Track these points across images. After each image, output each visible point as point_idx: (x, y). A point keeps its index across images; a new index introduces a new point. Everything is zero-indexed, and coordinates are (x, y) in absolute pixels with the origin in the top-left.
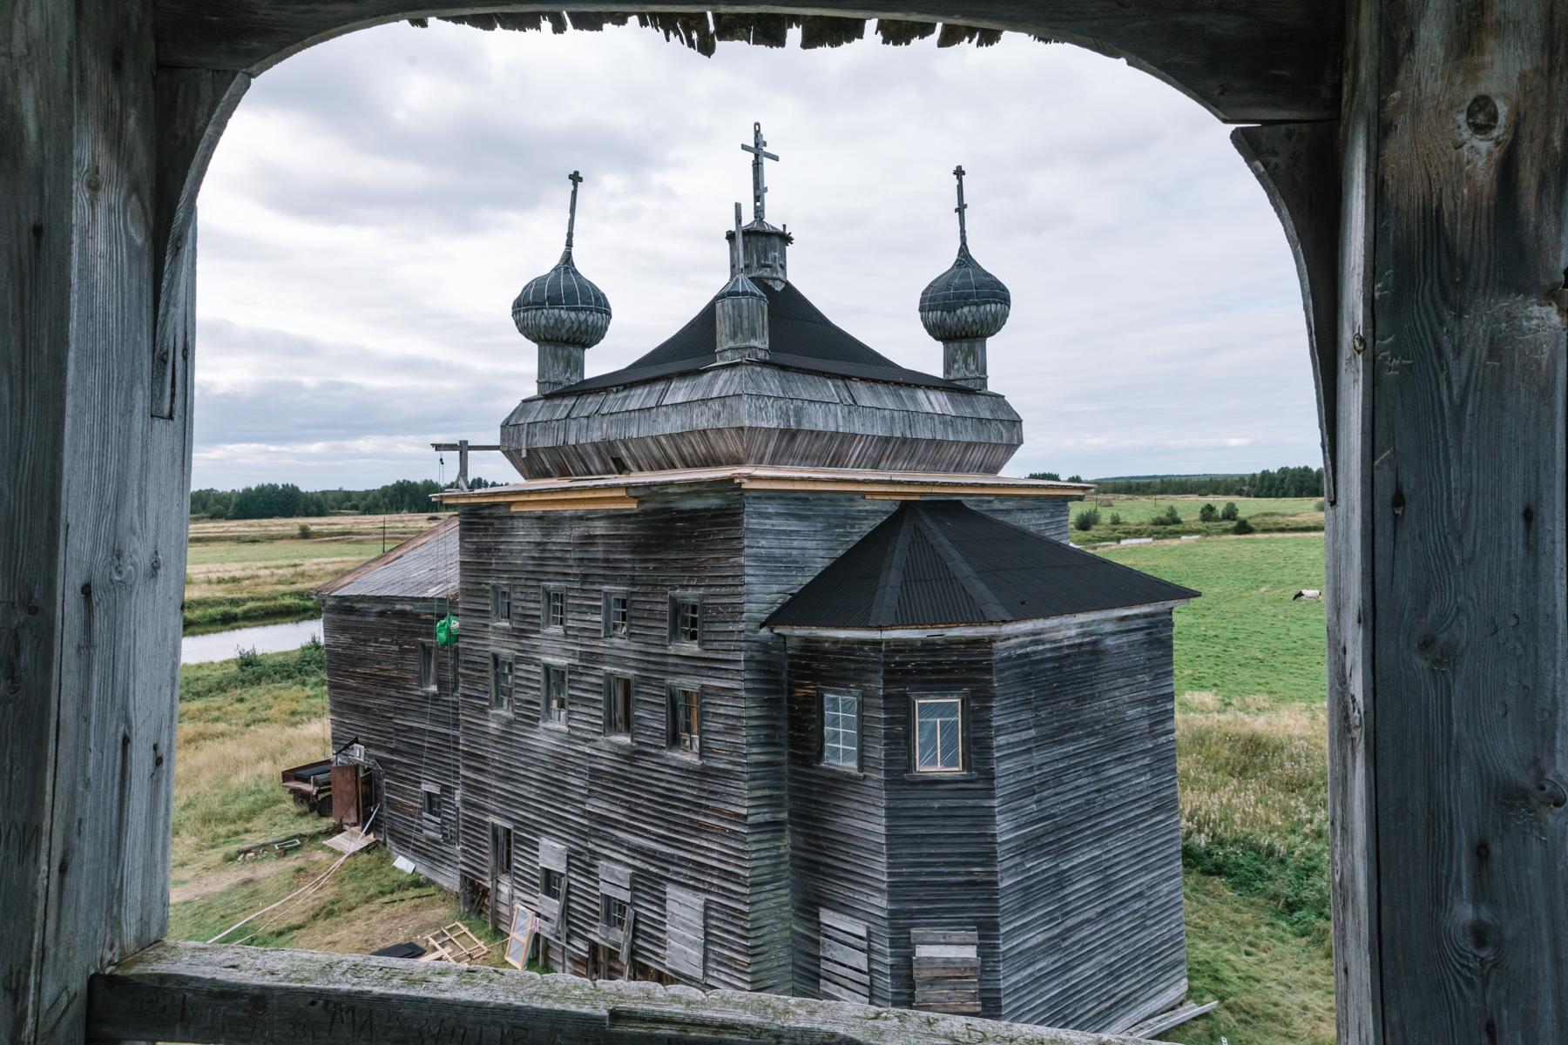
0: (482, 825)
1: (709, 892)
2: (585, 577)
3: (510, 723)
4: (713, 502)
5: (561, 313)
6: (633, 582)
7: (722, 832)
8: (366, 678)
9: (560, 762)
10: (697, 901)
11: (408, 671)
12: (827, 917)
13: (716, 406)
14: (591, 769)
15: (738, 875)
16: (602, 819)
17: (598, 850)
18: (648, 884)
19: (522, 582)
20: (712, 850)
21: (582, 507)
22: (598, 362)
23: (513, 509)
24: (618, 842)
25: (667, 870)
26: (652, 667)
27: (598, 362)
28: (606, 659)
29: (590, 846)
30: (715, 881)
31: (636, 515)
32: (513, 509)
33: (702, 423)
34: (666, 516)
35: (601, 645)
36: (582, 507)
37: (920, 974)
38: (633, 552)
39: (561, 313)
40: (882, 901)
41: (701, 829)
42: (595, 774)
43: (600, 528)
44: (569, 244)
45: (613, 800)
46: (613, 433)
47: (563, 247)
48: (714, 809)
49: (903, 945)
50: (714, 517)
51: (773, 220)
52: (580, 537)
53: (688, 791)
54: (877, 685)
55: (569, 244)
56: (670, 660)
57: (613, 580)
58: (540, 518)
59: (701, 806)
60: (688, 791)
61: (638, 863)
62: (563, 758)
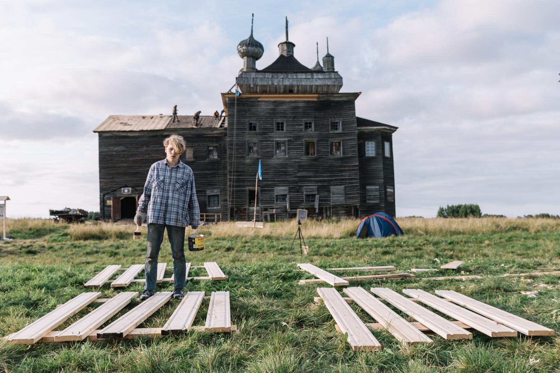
0: (244, 191)
2: (294, 117)
4: (345, 99)
5: (252, 49)
6: (315, 117)
7: (350, 170)
8: (136, 162)
9: (284, 166)
10: (343, 186)
12: (368, 187)
13: (334, 80)
18: (324, 188)
20: (346, 175)
21: (293, 100)
22: (261, 64)
23: (259, 99)
24: (311, 181)
27: (261, 64)
32: (259, 99)
33: (329, 83)
35: (302, 134)
37: (388, 194)
39: (252, 49)
40: (382, 180)
41: (345, 171)
42: (300, 166)
43: (301, 105)
44: (252, 32)
45: (309, 171)
46: (295, 83)
47: (250, 33)
49: (386, 188)
51: (290, 40)
54: (380, 138)
55: (252, 32)
57: (308, 117)
60: (338, 164)
62: (286, 164)
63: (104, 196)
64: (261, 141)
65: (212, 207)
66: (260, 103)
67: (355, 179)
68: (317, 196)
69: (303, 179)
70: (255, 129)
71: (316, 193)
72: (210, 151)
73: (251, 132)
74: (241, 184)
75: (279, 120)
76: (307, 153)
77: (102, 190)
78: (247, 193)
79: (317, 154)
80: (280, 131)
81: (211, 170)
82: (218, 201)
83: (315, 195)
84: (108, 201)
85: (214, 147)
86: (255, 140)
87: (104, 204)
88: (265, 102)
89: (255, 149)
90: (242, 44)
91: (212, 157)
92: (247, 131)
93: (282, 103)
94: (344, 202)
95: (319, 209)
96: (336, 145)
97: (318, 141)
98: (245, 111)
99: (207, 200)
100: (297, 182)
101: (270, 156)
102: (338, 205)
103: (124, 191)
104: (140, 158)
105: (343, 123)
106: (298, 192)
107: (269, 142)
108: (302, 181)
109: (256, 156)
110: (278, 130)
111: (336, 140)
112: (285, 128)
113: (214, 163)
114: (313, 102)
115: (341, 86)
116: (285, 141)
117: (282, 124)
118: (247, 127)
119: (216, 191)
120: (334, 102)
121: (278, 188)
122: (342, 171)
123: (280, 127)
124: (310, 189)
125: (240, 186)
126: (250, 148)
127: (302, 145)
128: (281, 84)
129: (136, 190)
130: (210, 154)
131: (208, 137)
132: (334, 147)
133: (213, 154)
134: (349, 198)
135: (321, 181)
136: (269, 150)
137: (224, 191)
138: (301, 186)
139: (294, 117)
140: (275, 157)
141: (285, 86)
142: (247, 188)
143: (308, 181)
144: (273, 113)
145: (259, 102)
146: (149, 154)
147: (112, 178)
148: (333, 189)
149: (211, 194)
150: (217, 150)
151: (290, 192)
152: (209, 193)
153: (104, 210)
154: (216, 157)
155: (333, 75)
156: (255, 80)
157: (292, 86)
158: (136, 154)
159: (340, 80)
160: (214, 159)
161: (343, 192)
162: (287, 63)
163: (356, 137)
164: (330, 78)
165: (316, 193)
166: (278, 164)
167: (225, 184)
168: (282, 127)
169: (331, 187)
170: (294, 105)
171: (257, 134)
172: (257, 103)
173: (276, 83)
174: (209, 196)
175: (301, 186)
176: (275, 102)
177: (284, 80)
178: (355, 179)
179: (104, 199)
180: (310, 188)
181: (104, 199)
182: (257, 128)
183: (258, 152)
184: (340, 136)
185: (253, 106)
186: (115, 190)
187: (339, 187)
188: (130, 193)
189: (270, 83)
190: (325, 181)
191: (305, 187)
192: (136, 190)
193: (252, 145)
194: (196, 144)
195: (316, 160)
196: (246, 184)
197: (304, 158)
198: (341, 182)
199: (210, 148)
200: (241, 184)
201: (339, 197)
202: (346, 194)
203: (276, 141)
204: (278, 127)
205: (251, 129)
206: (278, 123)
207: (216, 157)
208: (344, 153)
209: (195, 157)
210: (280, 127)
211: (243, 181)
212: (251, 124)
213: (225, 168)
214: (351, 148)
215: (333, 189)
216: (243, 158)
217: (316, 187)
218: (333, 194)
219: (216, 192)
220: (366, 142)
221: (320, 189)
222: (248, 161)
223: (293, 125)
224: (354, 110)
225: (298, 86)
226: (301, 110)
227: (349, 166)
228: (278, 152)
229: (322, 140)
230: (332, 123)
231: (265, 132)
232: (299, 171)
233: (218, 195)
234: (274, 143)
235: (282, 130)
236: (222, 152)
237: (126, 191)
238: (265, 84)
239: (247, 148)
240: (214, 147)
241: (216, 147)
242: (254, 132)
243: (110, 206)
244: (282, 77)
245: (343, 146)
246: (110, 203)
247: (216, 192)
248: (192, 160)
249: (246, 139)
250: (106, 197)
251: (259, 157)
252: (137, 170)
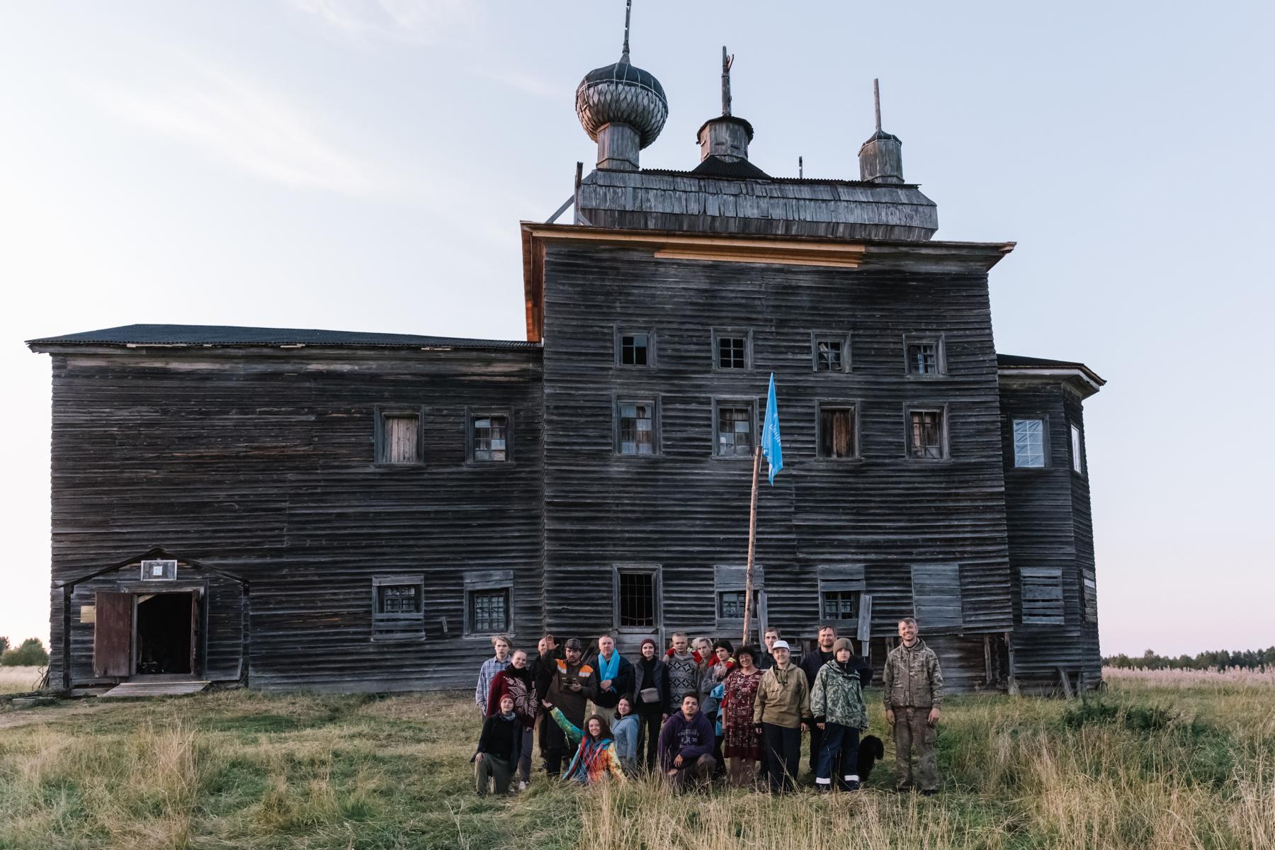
1: (960, 559)
2: (782, 323)
3: (653, 463)
4: (952, 268)
6: (854, 326)
10: (955, 566)
11: (341, 445)
14: (797, 489)
15: (995, 538)
16: (815, 529)
17: (813, 557)
19: (675, 326)
20: (965, 526)
21: (777, 262)
25: (911, 553)
26: (885, 393)
28: (819, 391)
29: (801, 556)
30: (969, 549)
31: (857, 273)
33: (894, 220)
34: (899, 276)
36: (777, 262)
38: (852, 303)
39: (622, 105)
42: (803, 492)
43: (804, 281)
46: (777, 213)
48: (964, 495)
50: (953, 279)
52: (775, 287)
53: (934, 486)
56: (908, 387)
57: (828, 325)
58: (706, 267)
59: (950, 495)
60: (934, 486)
61: (873, 557)
63: (69, 587)
64: (666, 400)
65: (482, 631)
66: (662, 270)
67: (993, 541)
68: (866, 599)
69: (816, 537)
70: (642, 358)
71: (861, 586)
72: (478, 432)
73: (628, 366)
74: (593, 550)
75: (731, 331)
76: (827, 450)
77: (60, 564)
78: (616, 582)
79: (862, 451)
80: (732, 369)
81: (482, 500)
82: (507, 612)
83: (858, 593)
84: (84, 609)
85: (493, 419)
86: (646, 394)
87: (67, 620)
88: (679, 264)
89: (642, 426)
90: (595, 78)
91: (486, 457)
92: (617, 364)
93: (741, 272)
94: (959, 622)
95: (873, 643)
96: (922, 424)
97: (866, 406)
98: (608, 294)
99: (466, 609)
100: (793, 549)
101: (700, 451)
102: (938, 630)
103: (149, 573)
104: (214, 452)
105: (948, 347)
106: (797, 582)
107: (693, 406)
108: (811, 544)
109: (645, 450)
110: (725, 364)
111: (929, 404)
112: (749, 360)
113: (492, 474)
114: (847, 273)
115: (933, 231)
116: (749, 403)
117: (739, 343)
118: (618, 349)
119: (497, 575)
120: (915, 275)
121: (724, 567)
122: (949, 513)
123: (732, 354)
124: (840, 572)
125: (587, 558)
126: (628, 426)
127: (809, 417)
128: (730, 213)
129: (197, 568)
130: (477, 444)
131: (472, 384)
132: (917, 432)
133: (488, 444)
134: (977, 607)
135: (875, 546)
136: (692, 432)
137: (527, 575)
138: (807, 563)
139: (782, 323)
140: (714, 456)
141: (746, 221)
142: (616, 566)
143: (830, 544)
144: (708, 306)
145: (658, 263)
146: (251, 439)
147: (104, 524)
148: (922, 573)
149: (479, 587)
150: (503, 433)
151: (768, 582)
152: (472, 581)
153: (67, 643)
154: (501, 457)
155: (902, 196)
156: (640, 194)
157: (769, 221)
158: (200, 437)
159: (927, 210)
160: (493, 463)
161: (955, 584)
162: (727, 165)
163: (994, 399)
164: (896, 204)
165: (861, 586)
166: (725, 484)
167: (534, 553)
168: (739, 354)
169: (914, 567)
170: (779, 279)
171: (651, 376)
172: (652, 268)
173: (713, 210)
174: (474, 594)
175: (807, 563)
176: (714, 266)
177: (741, 200)
178: (993, 541)
179: (67, 598)
180: (840, 568)
181: (67, 598)
182: (652, 354)
183: (650, 438)
184: (941, 393)
185: (637, 277)
186: (115, 568)
187: (940, 567)
188: (172, 578)
189: (694, 208)
190: (891, 545)
191: (820, 567)
192: (197, 568)
193: (632, 414)
194: (426, 408)
195: (858, 471)
196: (610, 550)
197: (818, 463)
198: (946, 551)
199: (480, 424)
200: (593, 550)
201: (940, 602)
202: (965, 593)
203: (719, 402)
204: (725, 354)
205: (627, 358)
206: (725, 343)
207: (501, 457)
208: (954, 450)
209: (423, 451)
210: (732, 354)
211: (599, 540)
212: (628, 341)
213: (532, 494)
214: (980, 433)
215: (922, 573)
216: (601, 456)
217: (860, 566)
218: (920, 593)
219: (498, 578)
220: (1015, 421)
221: (874, 572)
222: (616, 469)
223: (775, 349)
224: (986, 304)
225: (788, 224)
226: (804, 299)
227: (971, 497)
228: (723, 440)
229: (878, 405)
230: (910, 347)
231: (678, 370)
232: (799, 510)
233: (507, 589)
234: (712, 407)
235: (740, 364)
236: (523, 438)
237: (158, 571)
238: (677, 211)
239: (615, 425)
240: (493, 419)
241: (500, 420)
242: (640, 367)
243: (88, 627)
244: (734, 190)
245: (952, 426)
246: (88, 613)
247: (498, 578)
248: (412, 463)
249: (613, 393)
250: (77, 591)
251: (659, 454)
252: (205, 497)
